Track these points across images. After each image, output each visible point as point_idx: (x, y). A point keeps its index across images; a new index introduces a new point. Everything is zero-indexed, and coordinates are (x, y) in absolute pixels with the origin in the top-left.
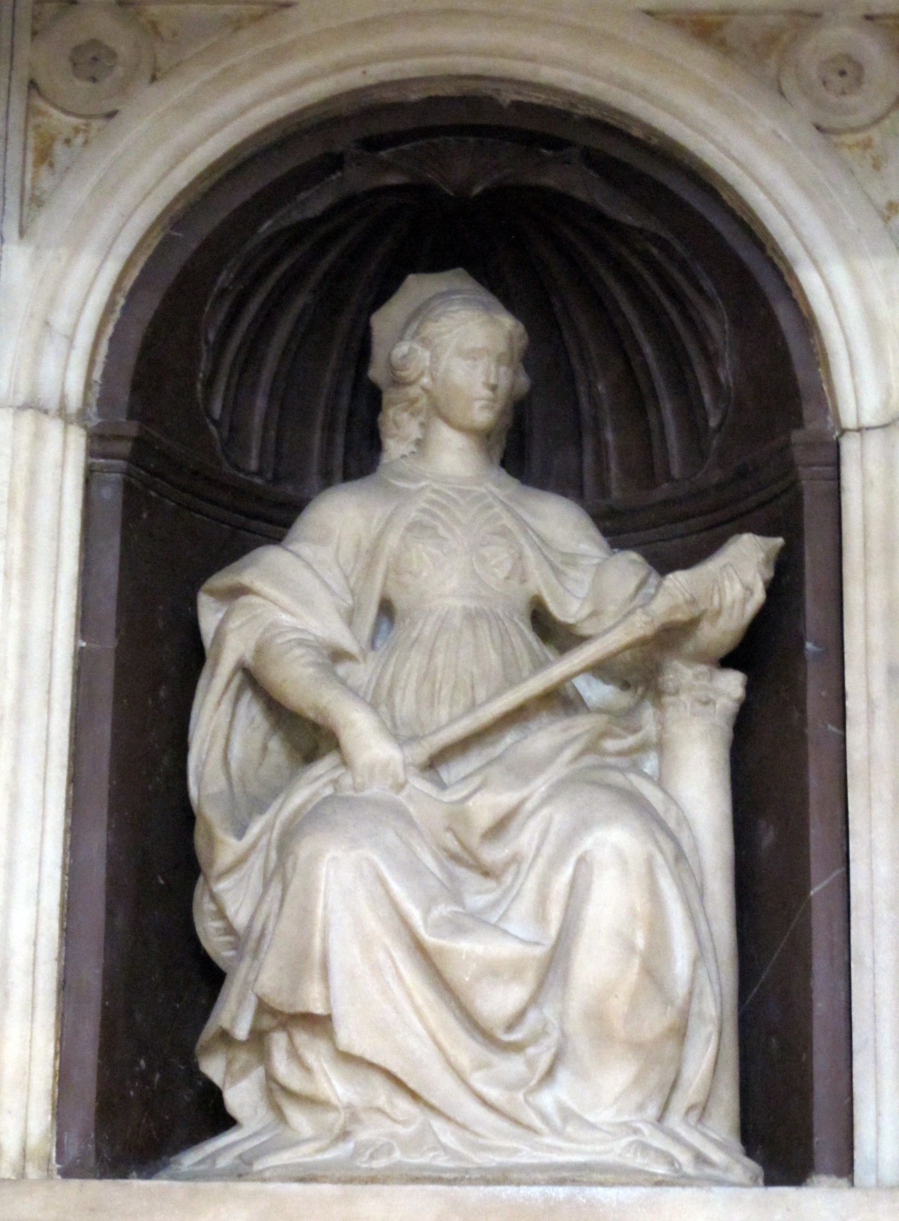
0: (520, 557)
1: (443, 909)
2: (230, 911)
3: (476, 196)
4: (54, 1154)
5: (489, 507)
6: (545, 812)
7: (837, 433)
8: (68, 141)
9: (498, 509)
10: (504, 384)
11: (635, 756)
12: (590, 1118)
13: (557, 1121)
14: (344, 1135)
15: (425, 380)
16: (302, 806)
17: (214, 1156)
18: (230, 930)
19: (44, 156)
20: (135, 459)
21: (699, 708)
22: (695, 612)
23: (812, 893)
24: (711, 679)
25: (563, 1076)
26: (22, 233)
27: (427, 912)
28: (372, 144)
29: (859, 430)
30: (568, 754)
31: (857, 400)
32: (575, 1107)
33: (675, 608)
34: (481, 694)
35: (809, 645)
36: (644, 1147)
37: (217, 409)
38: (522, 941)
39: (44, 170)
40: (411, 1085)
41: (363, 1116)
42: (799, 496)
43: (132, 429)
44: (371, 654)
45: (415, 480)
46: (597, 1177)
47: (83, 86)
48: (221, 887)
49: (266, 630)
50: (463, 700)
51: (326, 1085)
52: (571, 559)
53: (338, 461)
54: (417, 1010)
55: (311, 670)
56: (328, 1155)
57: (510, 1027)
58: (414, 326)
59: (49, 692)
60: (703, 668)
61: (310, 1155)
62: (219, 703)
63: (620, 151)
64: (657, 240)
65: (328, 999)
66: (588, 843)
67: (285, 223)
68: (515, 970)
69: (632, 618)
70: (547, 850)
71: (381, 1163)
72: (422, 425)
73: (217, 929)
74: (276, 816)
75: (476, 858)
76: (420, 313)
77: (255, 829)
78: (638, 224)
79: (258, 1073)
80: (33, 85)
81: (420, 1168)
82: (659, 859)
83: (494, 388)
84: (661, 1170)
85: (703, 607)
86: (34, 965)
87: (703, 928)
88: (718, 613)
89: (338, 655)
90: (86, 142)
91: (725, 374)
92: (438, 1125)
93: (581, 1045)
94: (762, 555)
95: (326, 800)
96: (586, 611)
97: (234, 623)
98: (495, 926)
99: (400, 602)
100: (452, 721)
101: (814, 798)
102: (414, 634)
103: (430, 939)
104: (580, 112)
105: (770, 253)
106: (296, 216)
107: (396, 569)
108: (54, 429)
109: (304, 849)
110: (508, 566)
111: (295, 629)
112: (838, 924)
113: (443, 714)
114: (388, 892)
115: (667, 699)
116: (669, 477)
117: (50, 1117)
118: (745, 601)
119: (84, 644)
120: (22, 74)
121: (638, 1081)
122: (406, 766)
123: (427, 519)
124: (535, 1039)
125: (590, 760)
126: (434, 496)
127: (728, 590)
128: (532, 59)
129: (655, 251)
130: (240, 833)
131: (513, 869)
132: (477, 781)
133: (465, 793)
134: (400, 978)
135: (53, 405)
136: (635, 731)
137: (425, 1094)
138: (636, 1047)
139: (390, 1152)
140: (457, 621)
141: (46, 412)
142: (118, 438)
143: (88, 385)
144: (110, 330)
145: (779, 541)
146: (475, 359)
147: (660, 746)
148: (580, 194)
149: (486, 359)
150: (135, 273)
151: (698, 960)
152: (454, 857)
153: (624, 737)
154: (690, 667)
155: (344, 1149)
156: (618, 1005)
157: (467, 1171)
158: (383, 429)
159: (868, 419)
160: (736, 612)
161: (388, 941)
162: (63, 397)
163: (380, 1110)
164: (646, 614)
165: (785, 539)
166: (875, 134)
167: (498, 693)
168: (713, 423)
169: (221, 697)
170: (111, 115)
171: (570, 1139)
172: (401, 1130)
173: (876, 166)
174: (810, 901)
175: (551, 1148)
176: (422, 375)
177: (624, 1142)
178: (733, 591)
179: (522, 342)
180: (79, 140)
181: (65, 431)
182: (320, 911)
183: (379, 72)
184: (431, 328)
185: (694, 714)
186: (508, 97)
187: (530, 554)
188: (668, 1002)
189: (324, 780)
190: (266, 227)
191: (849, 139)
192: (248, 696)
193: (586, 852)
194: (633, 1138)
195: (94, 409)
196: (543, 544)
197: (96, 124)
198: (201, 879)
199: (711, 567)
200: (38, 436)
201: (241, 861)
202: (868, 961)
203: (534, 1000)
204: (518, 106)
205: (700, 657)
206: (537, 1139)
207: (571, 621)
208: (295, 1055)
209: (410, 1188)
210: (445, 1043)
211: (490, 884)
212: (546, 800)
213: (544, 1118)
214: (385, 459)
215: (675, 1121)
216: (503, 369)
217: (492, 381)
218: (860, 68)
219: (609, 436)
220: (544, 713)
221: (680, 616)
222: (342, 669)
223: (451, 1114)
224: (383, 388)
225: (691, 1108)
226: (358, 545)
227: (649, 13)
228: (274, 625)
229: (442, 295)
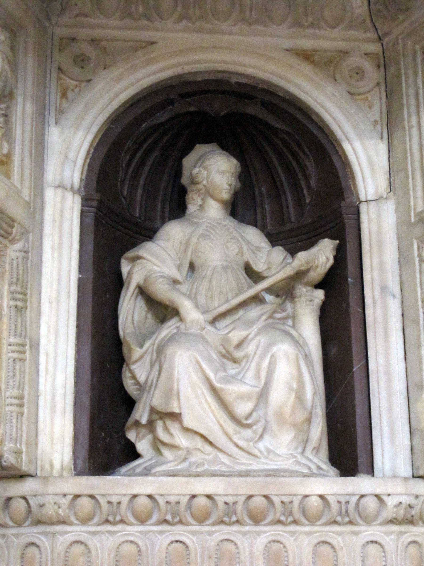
0: (241, 247)
1: (221, 374)
2: (138, 376)
3: (223, 116)
4: (73, 468)
5: (229, 229)
6: (257, 338)
7: (358, 203)
8: (73, 90)
9: (232, 230)
10: (234, 184)
11: (284, 321)
12: (278, 452)
13: (265, 453)
14: (185, 459)
15: (205, 182)
16: (165, 337)
17: (134, 468)
18: (137, 383)
19: (64, 95)
20: (98, 208)
21: (308, 302)
22: (309, 267)
23: (354, 370)
24: (312, 292)
25: (267, 437)
26: (56, 123)
27: (216, 375)
28: (183, 96)
29: (367, 201)
30: (264, 317)
31: (366, 191)
32: (271, 448)
33: (302, 265)
34: (230, 297)
35: (349, 279)
36: (299, 463)
37: (125, 192)
38: (251, 386)
39: (64, 100)
40: (211, 440)
41: (192, 452)
42: (344, 225)
43: (98, 196)
44: (187, 282)
45: (200, 219)
46: (282, 474)
47: (77, 70)
48: (133, 367)
49: (148, 272)
50: (223, 299)
51: (178, 440)
52: (259, 249)
53: (167, 214)
54: (212, 412)
55: (167, 286)
56: (180, 467)
57: (247, 418)
58: (200, 162)
59: (69, 293)
60: (309, 288)
61: (173, 467)
62: (130, 300)
63: (275, 101)
64: (288, 133)
65: (180, 407)
66: (274, 349)
67: (151, 124)
69: (286, 269)
70: (259, 352)
71: (200, 469)
72: (202, 199)
73: (132, 383)
74: (155, 340)
75: (232, 356)
76: (202, 158)
77: (147, 345)
78: (281, 128)
79: (150, 437)
80: (60, 69)
81: (216, 471)
82: (300, 357)
83: (230, 185)
84: (306, 471)
85: (311, 265)
86: (65, 395)
87: (315, 383)
88: (317, 267)
89: (175, 282)
90: (80, 90)
91: (313, 183)
92: (220, 455)
93: (273, 425)
94: (332, 246)
95: (174, 334)
96: (265, 268)
97: (136, 270)
98: (240, 380)
99: (197, 263)
100: (219, 306)
101: (353, 335)
102: (204, 274)
103: (218, 385)
104: (260, 86)
105: (330, 138)
106: (156, 122)
107: (195, 251)
108: (69, 195)
109: (169, 351)
110: (237, 250)
111: (159, 272)
112: (365, 381)
113: (216, 303)
114: (201, 368)
115: (296, 299)
116: (290, 222)
117: (72, 454)
118: (326, 263)
119: (81, 276)
120: (55, 66)
121: (296, 437)
122: (205, 321)
123: (207, 233)
124: (257, 422)
125: (270, 321)
126: (208, 225)
127: (320, 259)
128: (245, 66)
129: (287, 138)
131: (245, 360)
132: (231, 327)
133: (227, 331)
134: (206, 400)
135: (69, 186)
136: (284, 311)
137: (216, 444)
138: (294, 425)
139: (204, 465)
140: (219, 269)
141: (66, 189)
142: (93, 200)
143: (81, 180)
144: (88, 161)
145: (338, 242)
146: (223, 174)
147: (294, 317)
148: (260, 116)
149: (227, 174)
150: (97, 140)
151: (314, 394)
152: (224, 356)
153: (281, 313)
154: (304, 288)
155: (185, 465)
156: (287, 409)
157: (233, 472)
158: (187, 200)
159: (370, 198)
160: (323, 267)
161: (201, 385)
162: (72, 184)
163: (199, 450)
164: (291, 266)
165: (340, 241)
166: (369, 95)
167: (237, 295)
168: (307, 201)
169: (131, 298)
170: (89, 81)
171: (271, 460)
172: (207, 457)
173: (370, 107)
174: (353, 373)
175: (264, 463)
176: (203, 180)
177: (291, 461)
178: (322, 259)
179: (239, 169)
180: (77, 90)
181: (73, 197)
182: (176, 374)
183: (188, 69)
184: (207, 163)
185: (306, 305)
186: (234, 80)
187: (245, 247)
188: (305, 409)
189: (174, 326)
190: (144, 125)
191: (359, 97)
192: (140, 297)
193: (274, 353)
194: (294, 459)
195: (83, 189)
196: (249, 243)
197: (83, 84)
198: (125, 365)
199: (314, 250)
200: (63, 198)
201: (142, 357)
202: (377, 394)
203: (255, 409)
204: (237, 83)
205: (308, 284)
206: (258, 460)
207: (260, 271)
208: (166, 429)
209: (212, 478)
210: (223, 424)
211: (237, 365)
212: (256, 335)
213: (261, 452)
214: (188, 212)
215: (308, 453)
216: (233, 179)
217: (230, 183)
218: (363, 72)
219: (267, 207)
220: (253, 303)
221: (304, 268)
222: (178, 286)
223: (226, 451)
224: (187, 186)
225: (314, 448)
226: (181, 243)
227: (287, 50)
228: (150, 270)
229: (209, 152)
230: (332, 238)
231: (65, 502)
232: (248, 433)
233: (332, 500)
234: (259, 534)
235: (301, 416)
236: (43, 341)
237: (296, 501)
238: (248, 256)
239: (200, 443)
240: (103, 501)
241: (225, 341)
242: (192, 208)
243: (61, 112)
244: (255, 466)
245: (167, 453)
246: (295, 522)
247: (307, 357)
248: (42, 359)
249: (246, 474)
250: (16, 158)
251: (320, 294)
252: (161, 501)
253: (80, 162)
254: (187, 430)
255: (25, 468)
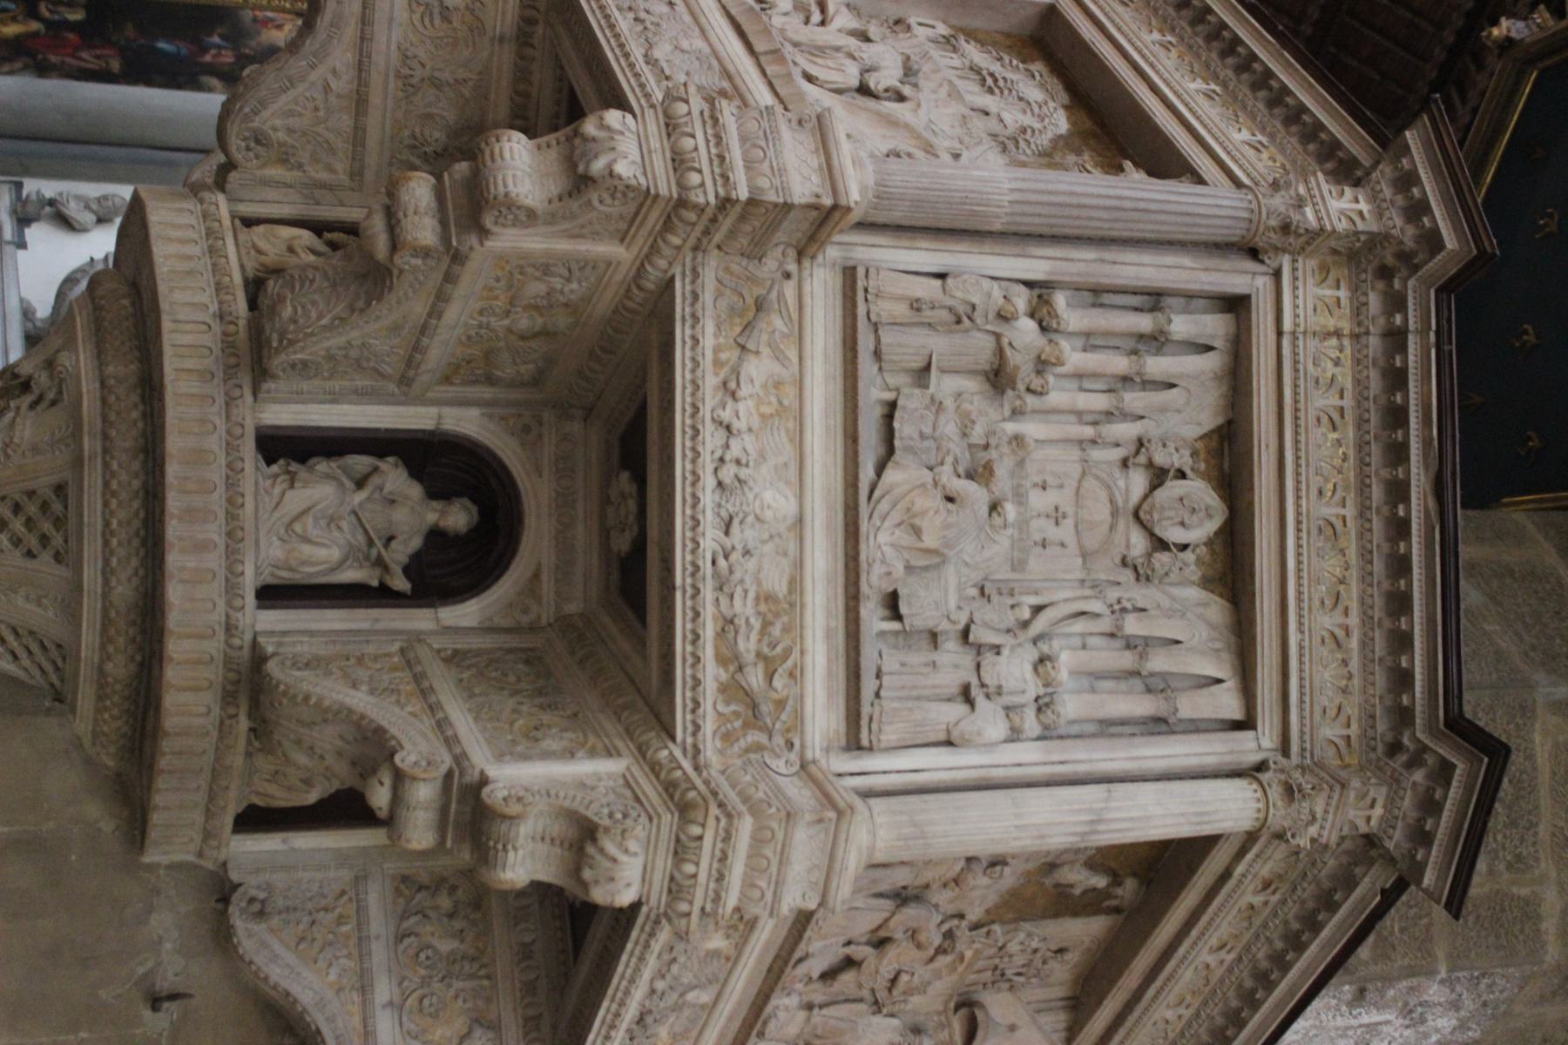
19: (502, 418)
68: (305, 530)
77: (339, 471)
89: (381, 490)
103: (312, 512)
130: (339, 467)
147: (361, 566)
155: (262, 491)
196: (410, 539)
199: (403, 578)
203: (298, 536)
215: (270, 568)
230: (413, 589)
231: (240, 419)
232: (282, 531)
233: (240, 579)
234: (220, 535)
235: (293, 563)
236: (339, 407)
237: (239, 557)
238: (401, 538)
239: (275, 500)
240: (239, 442)
241: (341, 518)
242: (434, 504)
243: (491, 417)
244: (262, 534)
245: (269, 482)
246: (227, 557)
247: (333, 570)
248: (327, 406)
249: (257, 529)
250: (451, 388)
251: (375, 583)
252: (240, 476)
253: (457, 429)
254: (283, 494)
255: (260, 396)
